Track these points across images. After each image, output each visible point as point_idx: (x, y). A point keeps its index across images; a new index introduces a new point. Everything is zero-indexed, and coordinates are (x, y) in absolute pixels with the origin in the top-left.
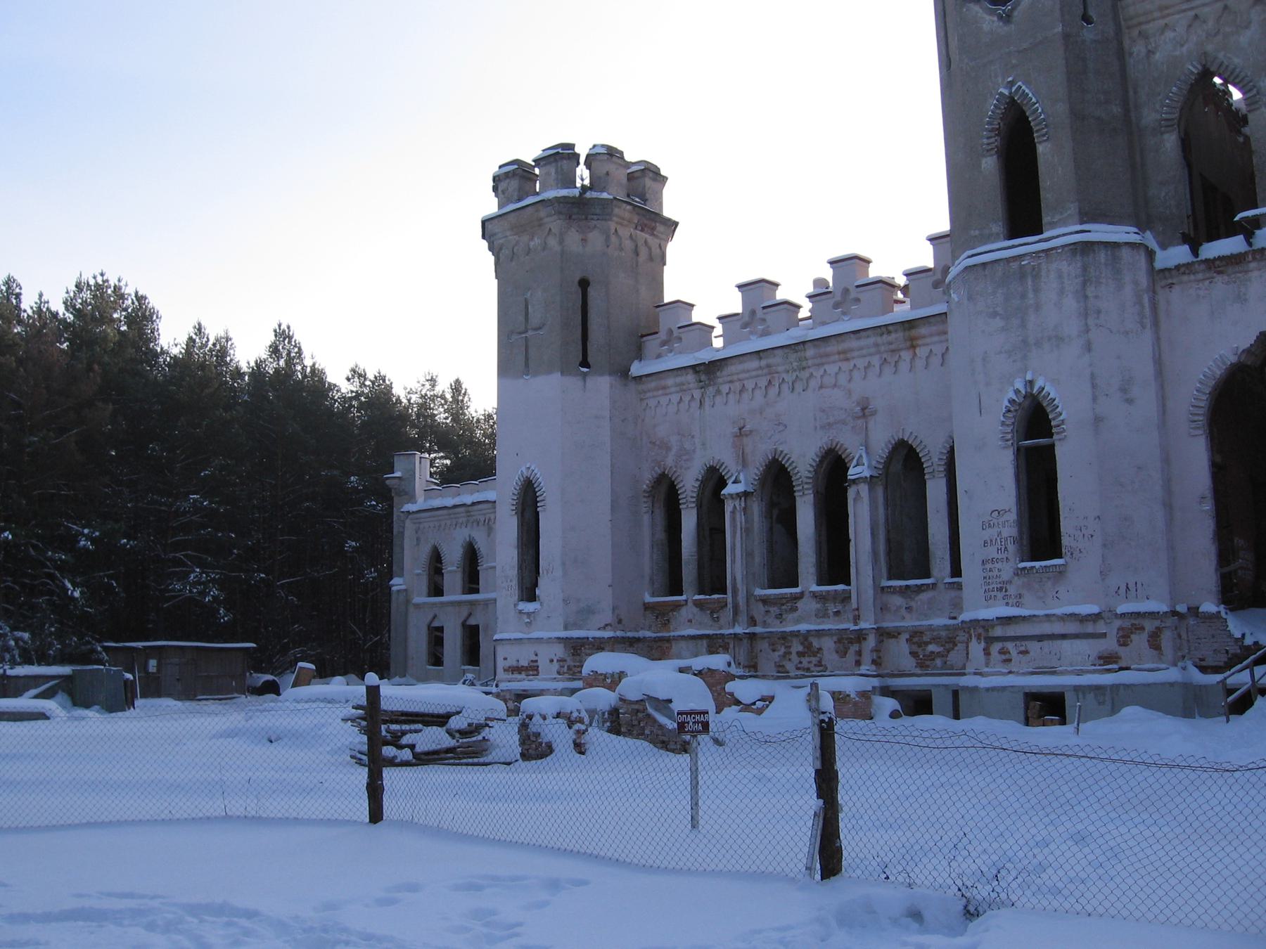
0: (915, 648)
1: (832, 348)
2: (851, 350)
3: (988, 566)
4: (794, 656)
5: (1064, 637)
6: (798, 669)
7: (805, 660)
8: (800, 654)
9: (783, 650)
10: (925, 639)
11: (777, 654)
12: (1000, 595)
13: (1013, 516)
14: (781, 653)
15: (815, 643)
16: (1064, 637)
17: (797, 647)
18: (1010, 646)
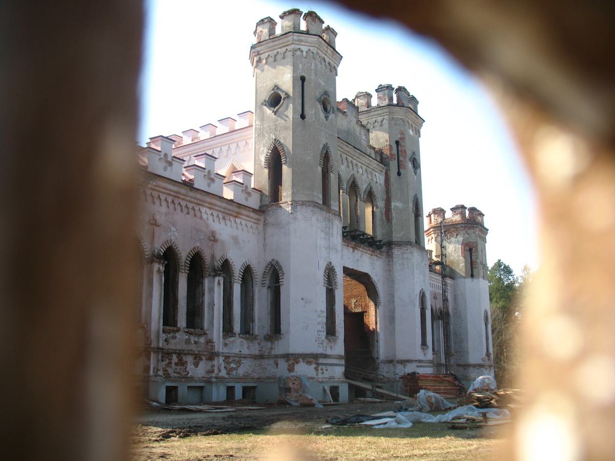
0: (226, 365)
1: (208, 199)
2: (215, 205)
3: (319, 333)
4: (173, 365)
5: (336, 365)
6: (175, 372)
7: (179, 367)
8: (176, 364)
9: (168, 361)
10: (230, 360)
11: (164, 363)
12: (322, 345)
13: (325, 314)
14: (166, 363)
15: (184, 358)
16: (336, 365)
17: (175, 359)
18: (323, 367)
